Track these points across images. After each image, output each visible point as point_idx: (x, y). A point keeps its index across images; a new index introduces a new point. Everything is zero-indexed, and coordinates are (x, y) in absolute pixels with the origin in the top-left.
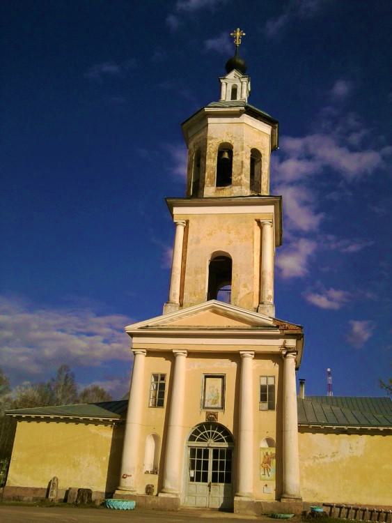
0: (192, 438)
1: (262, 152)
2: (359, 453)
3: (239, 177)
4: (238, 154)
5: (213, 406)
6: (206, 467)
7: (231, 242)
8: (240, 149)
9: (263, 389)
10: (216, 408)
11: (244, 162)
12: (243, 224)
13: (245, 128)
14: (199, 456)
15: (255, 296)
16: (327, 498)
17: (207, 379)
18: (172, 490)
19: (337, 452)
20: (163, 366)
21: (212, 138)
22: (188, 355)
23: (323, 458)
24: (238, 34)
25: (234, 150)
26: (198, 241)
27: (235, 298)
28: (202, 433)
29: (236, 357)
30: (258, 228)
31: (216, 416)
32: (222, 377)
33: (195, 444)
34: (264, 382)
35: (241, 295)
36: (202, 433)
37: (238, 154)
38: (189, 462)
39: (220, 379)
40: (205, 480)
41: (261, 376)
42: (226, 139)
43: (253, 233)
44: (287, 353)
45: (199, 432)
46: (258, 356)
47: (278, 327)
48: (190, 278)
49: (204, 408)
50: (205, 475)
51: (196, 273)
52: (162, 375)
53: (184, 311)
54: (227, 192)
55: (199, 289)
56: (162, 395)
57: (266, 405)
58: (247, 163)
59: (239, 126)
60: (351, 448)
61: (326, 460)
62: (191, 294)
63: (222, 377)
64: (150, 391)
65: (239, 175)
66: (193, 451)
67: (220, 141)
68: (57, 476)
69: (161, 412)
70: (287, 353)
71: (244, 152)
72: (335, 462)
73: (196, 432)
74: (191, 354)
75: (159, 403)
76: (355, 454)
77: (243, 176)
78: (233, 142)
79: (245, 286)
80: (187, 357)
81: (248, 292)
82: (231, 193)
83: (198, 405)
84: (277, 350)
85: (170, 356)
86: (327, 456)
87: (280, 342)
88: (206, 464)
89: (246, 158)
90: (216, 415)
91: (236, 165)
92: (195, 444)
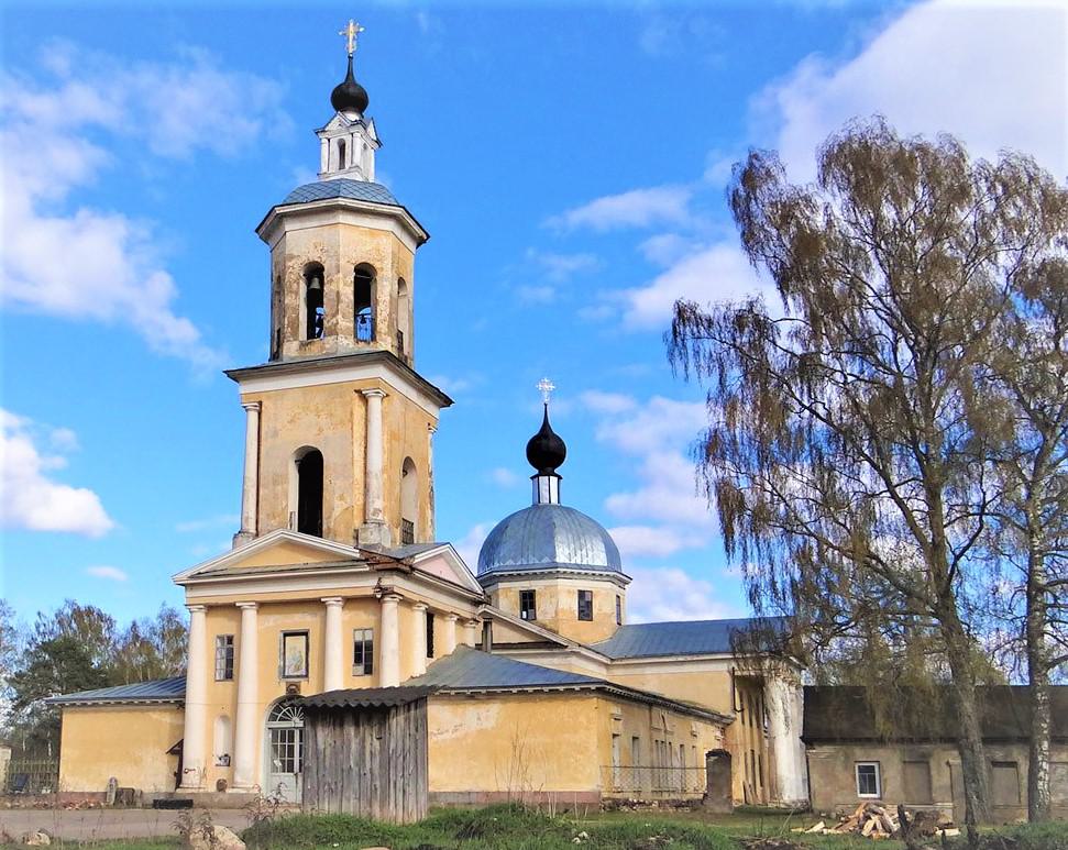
0: (273, 718)
1: (377, 265)
2: (489, 724)
3: (334, 320)
4: (332, 280)
5: (296, 674)
6: (291, 753)
7: (321, 430)
8: (334, 271)
9: (358, 647)
10: (298, 676)
11: (342, 291)
12: (337, 400)
13: (341, 230)
14: (283, 740)
15: (355, 512)
16: (446, 785)
17: (287, 638)
18: (242, 783)
19: (461, 725)
20: (225, 625)
21: (292, 257)
22: (345, 604)
23: (442, 733)
24: (351, 28)
25: (325, 274)
26: (275, 434)
27: (329, 517)
28: (280, 715)
29: (318, 604)
30: (361, 403)
31: (298, 687)
32: (306, 634)
33: (277, 724)
34: (359, 638)
35: (337, 512)
36: (280, 715)
37: (332, 280)
38: (270, 748)
39: (304, 637)
40: (291, 769)
41: (355, 630)
42: (315, 256)
43: (352, 413)
44: (383, 596)
45: (281, 708)
46: (349, 601)
47: (367, 560)
48: (266, 491)
49: (284, 677)
50: (291, 764)
51: (275, 483)
52: (228, 637)
53: (261, 539)
54: (316, 350)
55: (280, 508)
56: (230, 662)
57: (361, 669)
58: (348, 292)
59: (333, 228)
60: (479, 719)
61: (446, 736)
62: (268, 515)
63: (306, 634)
64: (216, 659)
65: (334, 316)
66: (274, 731)
67: (305, 259)
68: (117, 777)
69: (229, 684)
70: (383, 596)
71: (341, 275)
72: (458, 739)
73: (277, 709)
74: (263, 606)
75: (229, 676)
76: (483, 727)
77: (339, 316)
78: (323, 259)
79: (342, 498)
80: (258, 611)
81: (345, 506)
82: (322, 348)
83: (276, 672)
84: (370, 592)
85: (233, 609)
86: (447, 731)
87: (373, 582)
88: (291, 748)
89: (345, 284)
90: (298, 686)
91: (329, 300)
92: (277, 724)
